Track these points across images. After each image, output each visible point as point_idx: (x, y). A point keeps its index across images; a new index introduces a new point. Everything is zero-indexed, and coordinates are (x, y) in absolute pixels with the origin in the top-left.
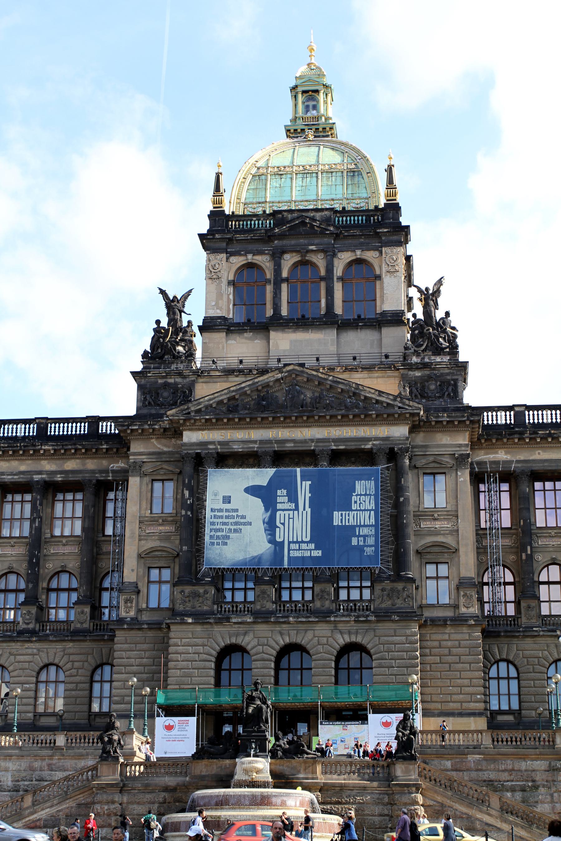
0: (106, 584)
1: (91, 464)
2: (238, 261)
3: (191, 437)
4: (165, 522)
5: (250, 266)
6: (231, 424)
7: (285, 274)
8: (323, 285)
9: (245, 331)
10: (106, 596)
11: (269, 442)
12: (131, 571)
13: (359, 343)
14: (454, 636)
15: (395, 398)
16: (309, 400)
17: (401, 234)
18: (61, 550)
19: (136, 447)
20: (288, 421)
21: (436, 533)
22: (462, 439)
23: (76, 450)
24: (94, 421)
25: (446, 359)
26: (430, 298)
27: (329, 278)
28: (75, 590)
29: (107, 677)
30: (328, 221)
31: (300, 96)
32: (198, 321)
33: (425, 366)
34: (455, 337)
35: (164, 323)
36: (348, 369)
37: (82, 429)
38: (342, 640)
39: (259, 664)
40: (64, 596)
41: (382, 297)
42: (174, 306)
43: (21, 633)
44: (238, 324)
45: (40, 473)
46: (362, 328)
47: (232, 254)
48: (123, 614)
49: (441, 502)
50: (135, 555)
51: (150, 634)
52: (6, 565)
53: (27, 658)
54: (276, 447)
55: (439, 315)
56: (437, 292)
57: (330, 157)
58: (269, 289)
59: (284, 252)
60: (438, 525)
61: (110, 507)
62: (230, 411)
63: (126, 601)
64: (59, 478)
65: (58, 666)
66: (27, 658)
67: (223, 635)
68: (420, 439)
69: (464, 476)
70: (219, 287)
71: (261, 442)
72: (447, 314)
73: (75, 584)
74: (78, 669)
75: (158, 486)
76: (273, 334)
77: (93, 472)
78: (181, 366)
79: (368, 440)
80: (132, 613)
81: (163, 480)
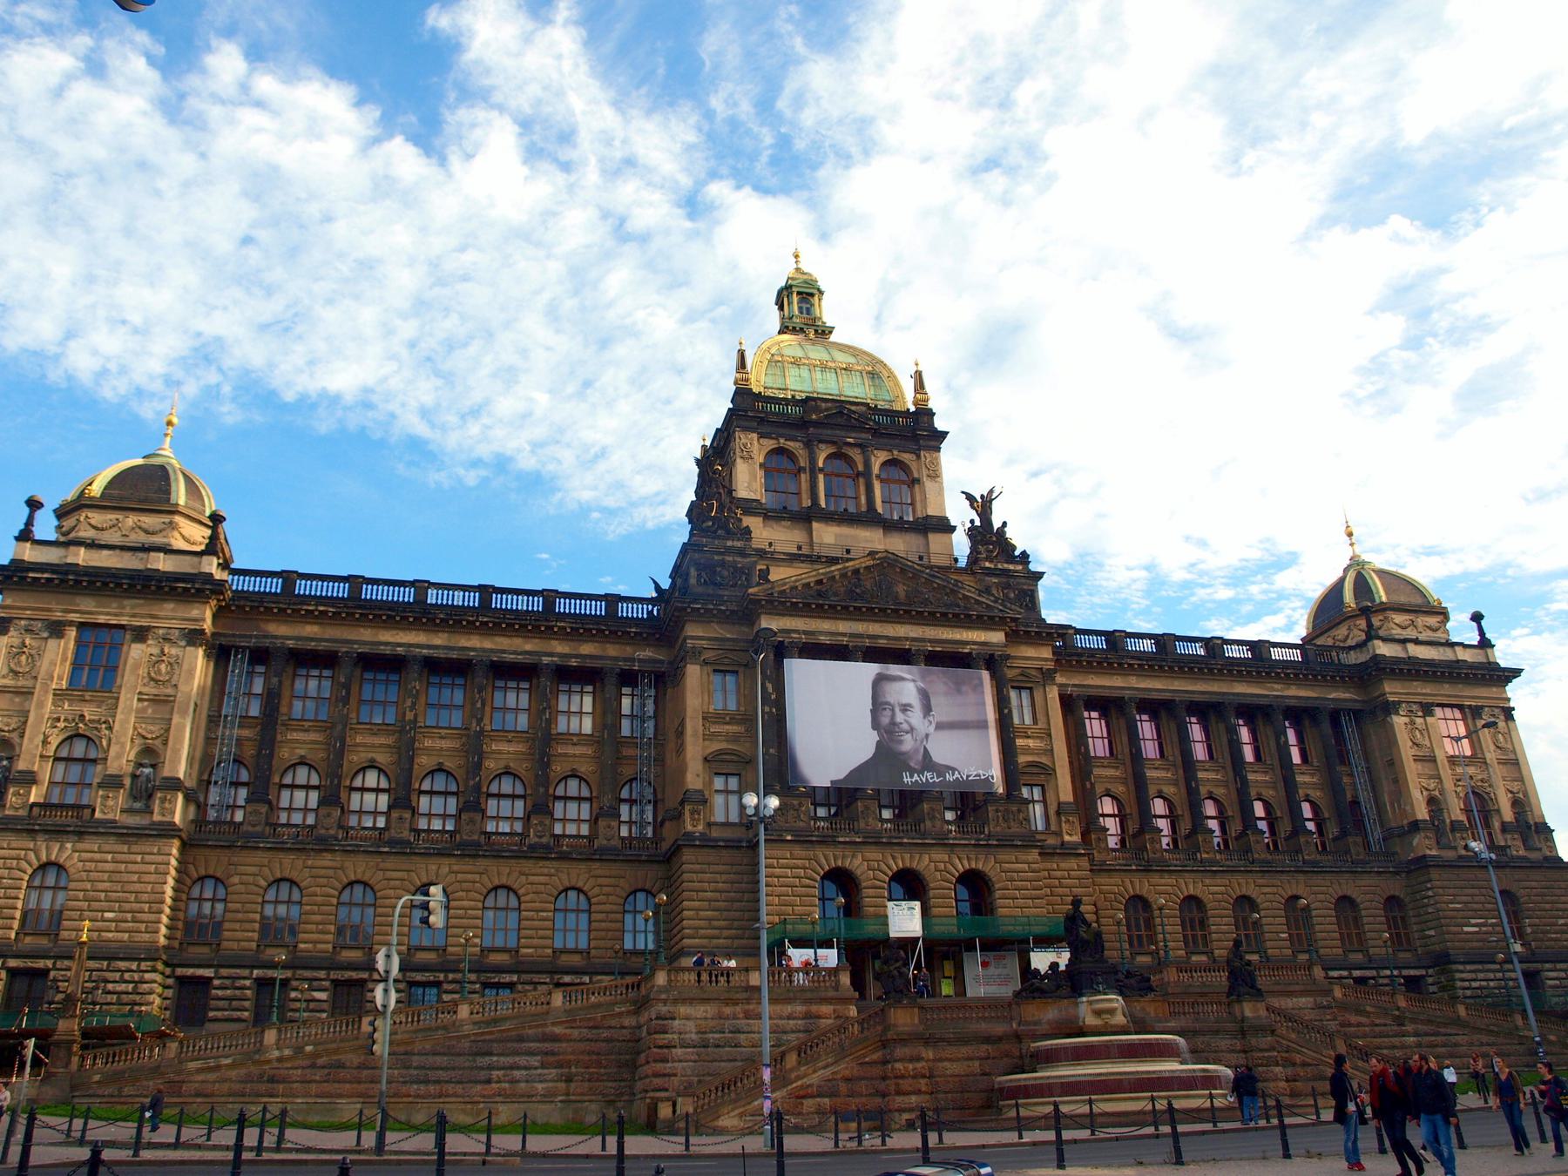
0: (625, 794)
1: (612, 650)
2: (770, 444)
3: (766, 622)
4: (733, 720)
5: (779, 451)
6: (820, 611)
7: (821, 464)
8: (861, 480)
9: (783, 519)
10: (624, 809)
11: (860, 636)
12: (694, 776)
14: (1063, 865)
16: (902, 594)
18: (571, 750)
19: (694, 632)
20: (883, 615)
22: (1046, 653)
23: (598, 631)
24: (612, 600)
26: (983, 506)
27: (867, 474)
28: (590, 799)
29: (640, 905)
34: (1014, 548)
37: (599, 609)
38: (961, 866)
39: (871, 892)
40: (572, 808)
41: (924, 499)
43: (532, 847)
44: (774, 511)
45: (551, 655)
46: (907, 530)
47: (761, 436)
48: (689, 828)
49: (1028, 720)
50: (700, 758)
51: (724, 852)
52: (502, 764)
53: (542, 879)
54: (867, 643)
58: (804, 477)
59: (820, 441)
61: (626, 702)
62: (820, 594)
63: (692, 814)
64: (574, 663)
65: (580, 890)
66: (542, 879)
67: (828, 858)
69: (1053, 694)
71: (852, 635)
72: (1005, 524)
73: (585, 793)
74: (608, 895)
75: (717, 678)
76: (815, 525)
77: (616, 659)
78: (738, 544)
79: (967, 643)
80: (700, 828)
81: (724, 672)
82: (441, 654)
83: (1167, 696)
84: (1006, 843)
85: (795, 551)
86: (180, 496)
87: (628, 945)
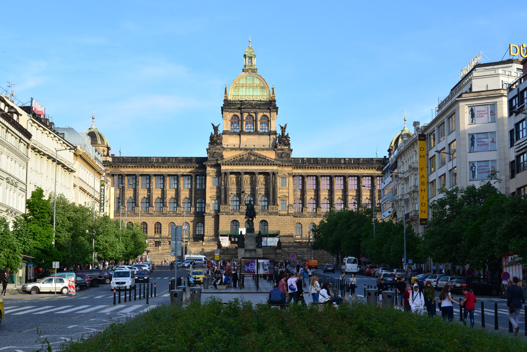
0: (198, 201)
2: (232, 114)
10: (198, 204)
13: (265, 141)
15: (275, 159)
17: (276, 109)
21: (284, 193)
25: (287, 147)
26: (283, 129)
27: (256, 121)
29: (200, 226)
30: (256, 104)
31: (247, 58)
32: (222, 132)
33: (282, 150)
35: (213, 133)
36: (263, 150)
42: (216, 129)
55: (286, 134)
56: (285, 128)
57: (257, 82)
60: (284, 191)
64: (185, 174)
67: (233, 218)
68: (280, 169)
69: (291, 179)
70: (227, 122)
76: (241, 136)
78: (219, 147)
82: (157, 173)
83: (329, 174)
84: (271, 214)
85: (233, 147)
86: (99, 142)
87: (197, 233)
